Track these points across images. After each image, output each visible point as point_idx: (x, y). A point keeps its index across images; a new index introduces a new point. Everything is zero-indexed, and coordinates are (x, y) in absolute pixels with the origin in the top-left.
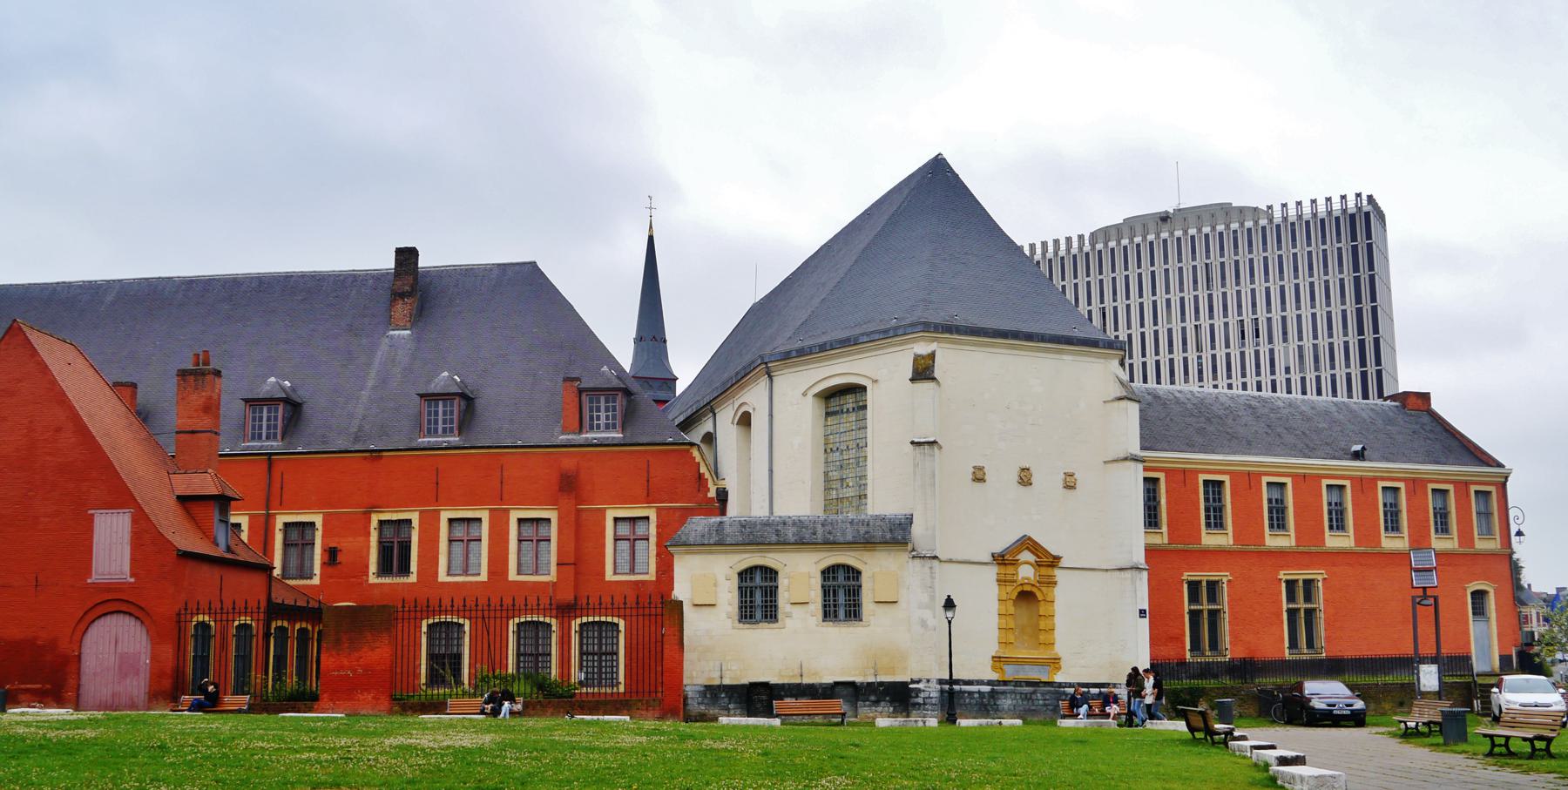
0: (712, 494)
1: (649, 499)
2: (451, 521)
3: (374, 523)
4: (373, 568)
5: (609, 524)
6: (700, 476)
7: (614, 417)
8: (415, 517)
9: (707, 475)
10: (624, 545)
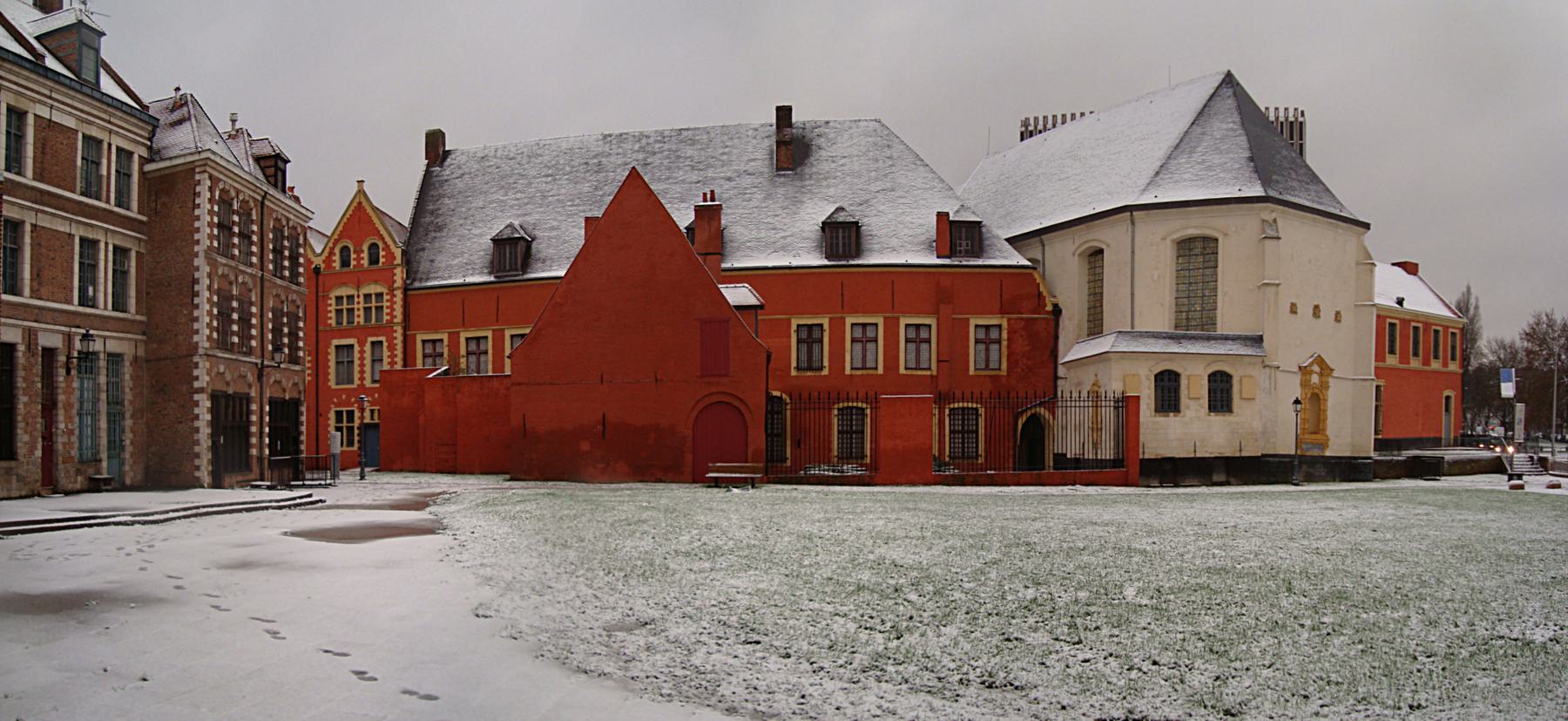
0: (1049, 308)
1: (1002, 312)
2: (853, 325)
3: (794, 327)
4: (794, 364)
5: (972, 329)
6: (1040, 294)
7: (972, 246)
8: (825, 322)
9: (1045, 294)
10: (982, 347)
